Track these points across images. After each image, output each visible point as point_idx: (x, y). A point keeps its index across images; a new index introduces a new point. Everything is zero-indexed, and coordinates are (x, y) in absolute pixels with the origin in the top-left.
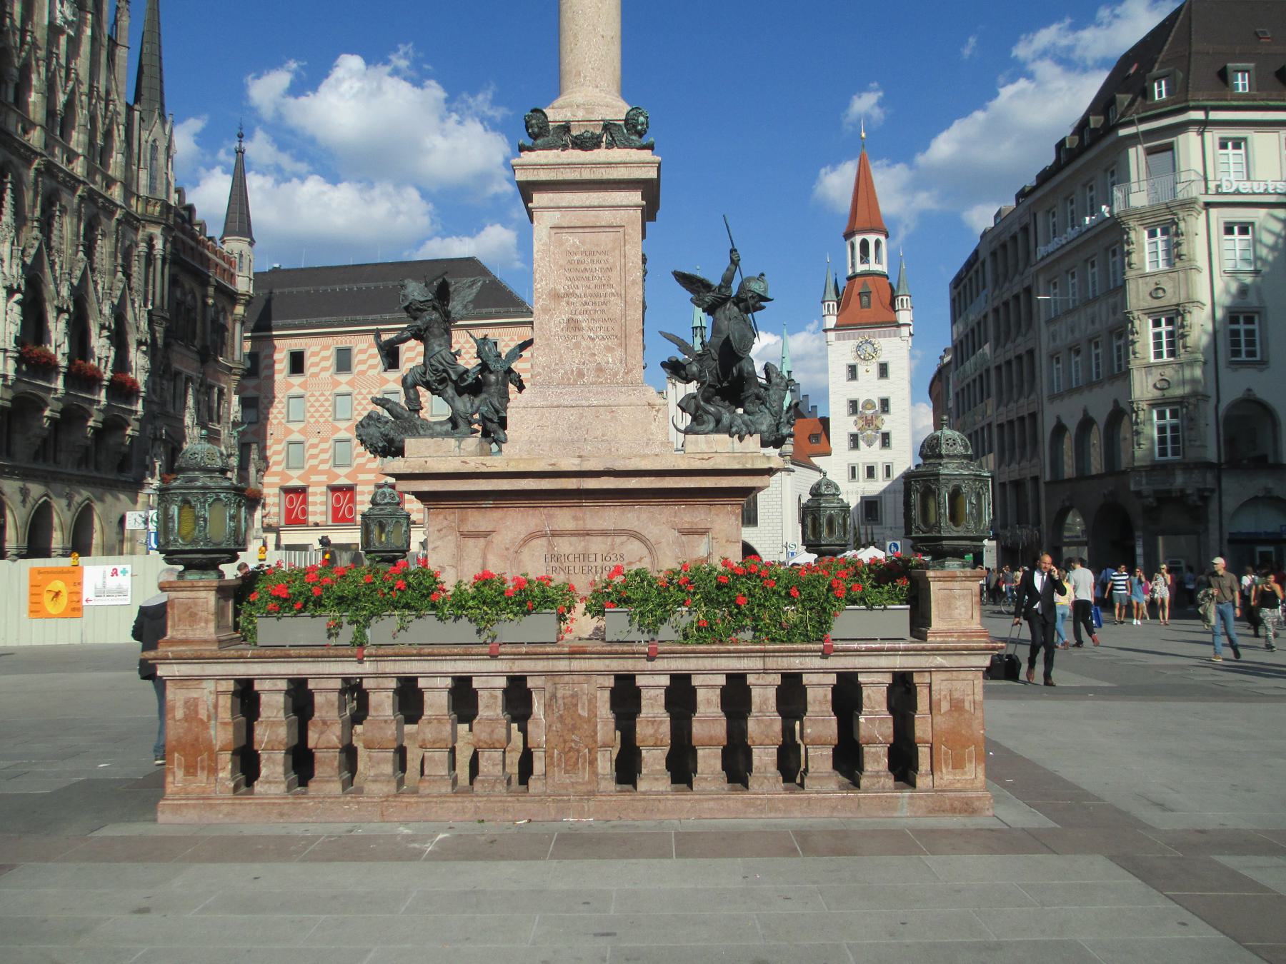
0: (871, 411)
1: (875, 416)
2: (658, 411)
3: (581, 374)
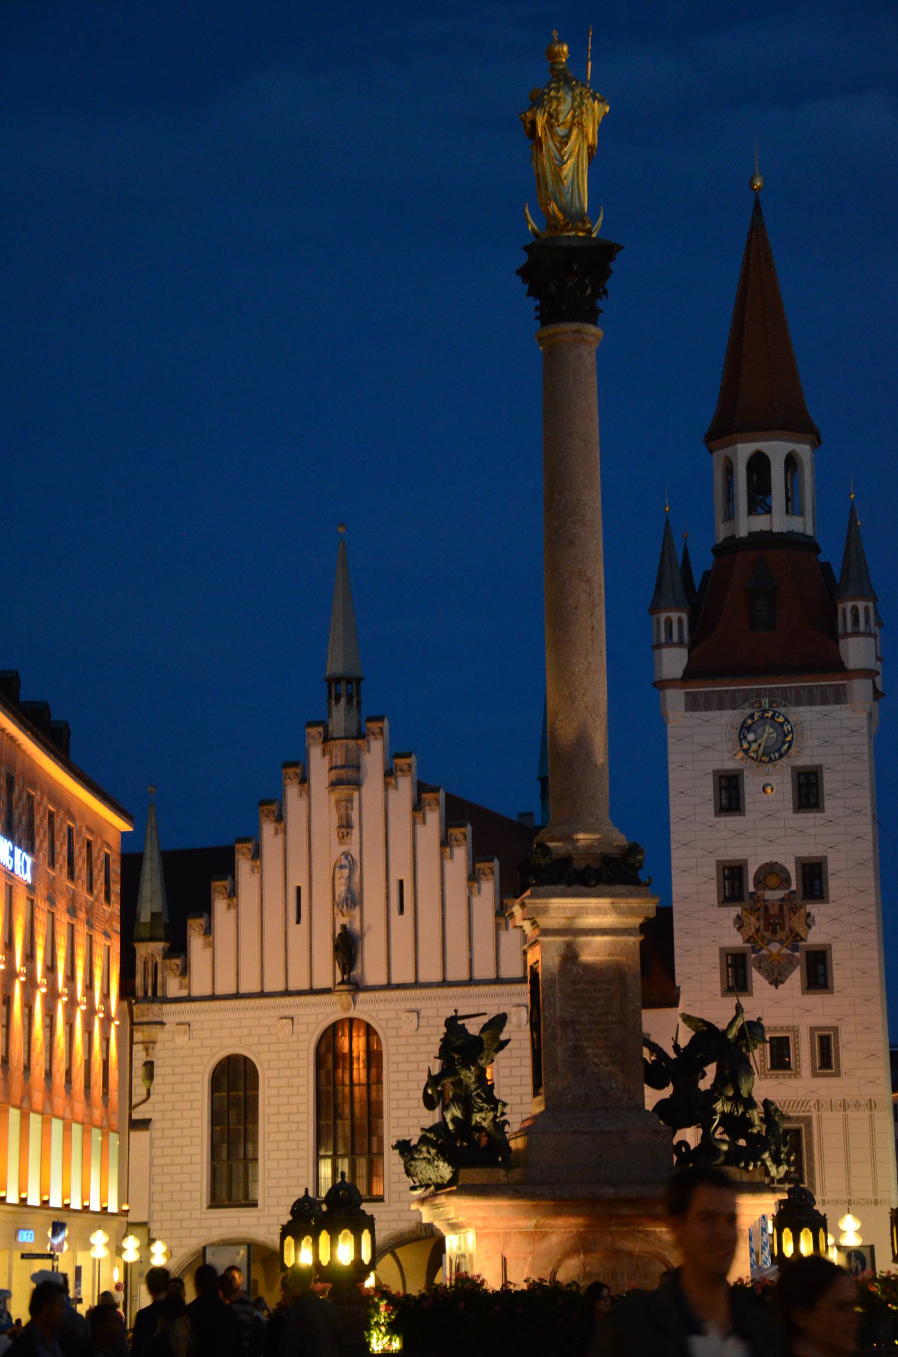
0: (779, 894)
1: (790, 905)
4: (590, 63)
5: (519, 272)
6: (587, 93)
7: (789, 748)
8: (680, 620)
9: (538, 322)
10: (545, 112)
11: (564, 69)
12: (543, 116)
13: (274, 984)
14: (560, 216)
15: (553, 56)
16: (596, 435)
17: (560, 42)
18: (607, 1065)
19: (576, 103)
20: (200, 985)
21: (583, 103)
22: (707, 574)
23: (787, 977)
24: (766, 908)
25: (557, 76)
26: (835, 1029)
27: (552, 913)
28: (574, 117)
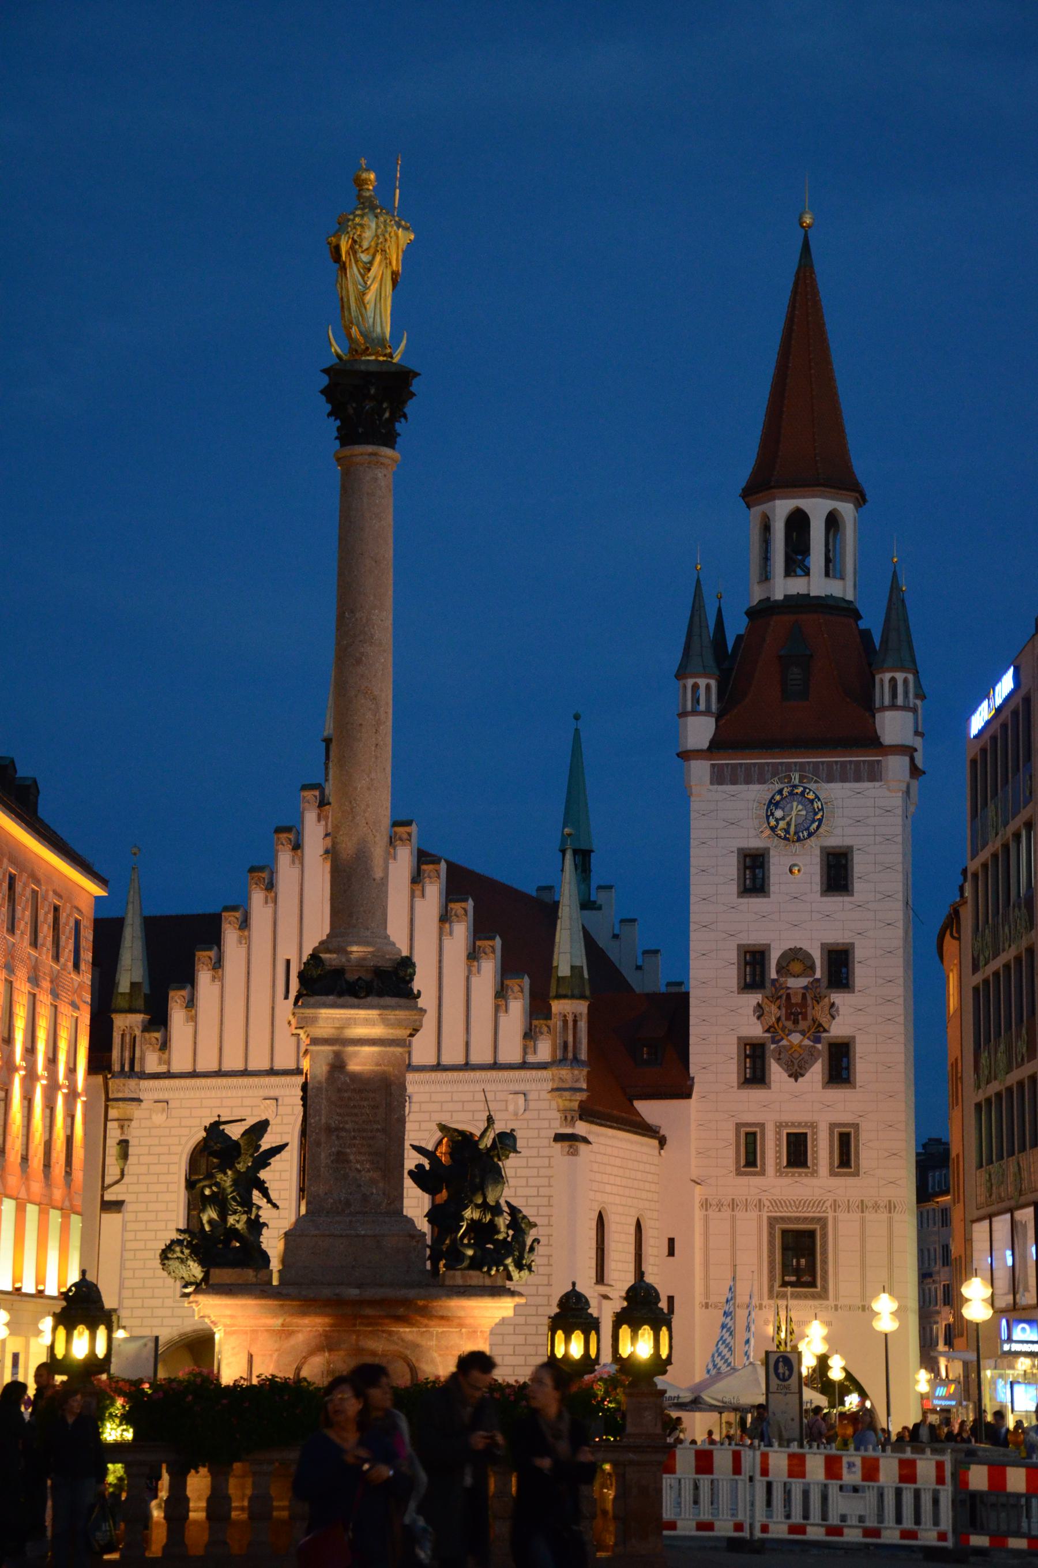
0: (803, 981)
1: (814, 994)
2: (418, 1242)
3: (348, 1203)
4: (398, 191)
5: (322, 392)
6: (391, 221)
7: (818, 827)
8: (708, 687)
9: (338, 442)
10: (349, 238)
11: (371, 196)
12: (348, 242)
13: (259, 1062)
14: (361, 340)
15: (360, 183)
16: (390, 554)
17: (367, 170)
18: (369, 1171)
19: (380, 231)
20: (180, 1062)
21: (386, 231)
22: (739, 638)
23: (807, 1070)
24: (788, 996)
25: (363, 203)
26: (856, 1126)
27: (321, 1023)
28: (377, 245)
